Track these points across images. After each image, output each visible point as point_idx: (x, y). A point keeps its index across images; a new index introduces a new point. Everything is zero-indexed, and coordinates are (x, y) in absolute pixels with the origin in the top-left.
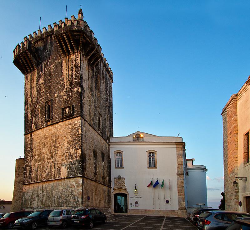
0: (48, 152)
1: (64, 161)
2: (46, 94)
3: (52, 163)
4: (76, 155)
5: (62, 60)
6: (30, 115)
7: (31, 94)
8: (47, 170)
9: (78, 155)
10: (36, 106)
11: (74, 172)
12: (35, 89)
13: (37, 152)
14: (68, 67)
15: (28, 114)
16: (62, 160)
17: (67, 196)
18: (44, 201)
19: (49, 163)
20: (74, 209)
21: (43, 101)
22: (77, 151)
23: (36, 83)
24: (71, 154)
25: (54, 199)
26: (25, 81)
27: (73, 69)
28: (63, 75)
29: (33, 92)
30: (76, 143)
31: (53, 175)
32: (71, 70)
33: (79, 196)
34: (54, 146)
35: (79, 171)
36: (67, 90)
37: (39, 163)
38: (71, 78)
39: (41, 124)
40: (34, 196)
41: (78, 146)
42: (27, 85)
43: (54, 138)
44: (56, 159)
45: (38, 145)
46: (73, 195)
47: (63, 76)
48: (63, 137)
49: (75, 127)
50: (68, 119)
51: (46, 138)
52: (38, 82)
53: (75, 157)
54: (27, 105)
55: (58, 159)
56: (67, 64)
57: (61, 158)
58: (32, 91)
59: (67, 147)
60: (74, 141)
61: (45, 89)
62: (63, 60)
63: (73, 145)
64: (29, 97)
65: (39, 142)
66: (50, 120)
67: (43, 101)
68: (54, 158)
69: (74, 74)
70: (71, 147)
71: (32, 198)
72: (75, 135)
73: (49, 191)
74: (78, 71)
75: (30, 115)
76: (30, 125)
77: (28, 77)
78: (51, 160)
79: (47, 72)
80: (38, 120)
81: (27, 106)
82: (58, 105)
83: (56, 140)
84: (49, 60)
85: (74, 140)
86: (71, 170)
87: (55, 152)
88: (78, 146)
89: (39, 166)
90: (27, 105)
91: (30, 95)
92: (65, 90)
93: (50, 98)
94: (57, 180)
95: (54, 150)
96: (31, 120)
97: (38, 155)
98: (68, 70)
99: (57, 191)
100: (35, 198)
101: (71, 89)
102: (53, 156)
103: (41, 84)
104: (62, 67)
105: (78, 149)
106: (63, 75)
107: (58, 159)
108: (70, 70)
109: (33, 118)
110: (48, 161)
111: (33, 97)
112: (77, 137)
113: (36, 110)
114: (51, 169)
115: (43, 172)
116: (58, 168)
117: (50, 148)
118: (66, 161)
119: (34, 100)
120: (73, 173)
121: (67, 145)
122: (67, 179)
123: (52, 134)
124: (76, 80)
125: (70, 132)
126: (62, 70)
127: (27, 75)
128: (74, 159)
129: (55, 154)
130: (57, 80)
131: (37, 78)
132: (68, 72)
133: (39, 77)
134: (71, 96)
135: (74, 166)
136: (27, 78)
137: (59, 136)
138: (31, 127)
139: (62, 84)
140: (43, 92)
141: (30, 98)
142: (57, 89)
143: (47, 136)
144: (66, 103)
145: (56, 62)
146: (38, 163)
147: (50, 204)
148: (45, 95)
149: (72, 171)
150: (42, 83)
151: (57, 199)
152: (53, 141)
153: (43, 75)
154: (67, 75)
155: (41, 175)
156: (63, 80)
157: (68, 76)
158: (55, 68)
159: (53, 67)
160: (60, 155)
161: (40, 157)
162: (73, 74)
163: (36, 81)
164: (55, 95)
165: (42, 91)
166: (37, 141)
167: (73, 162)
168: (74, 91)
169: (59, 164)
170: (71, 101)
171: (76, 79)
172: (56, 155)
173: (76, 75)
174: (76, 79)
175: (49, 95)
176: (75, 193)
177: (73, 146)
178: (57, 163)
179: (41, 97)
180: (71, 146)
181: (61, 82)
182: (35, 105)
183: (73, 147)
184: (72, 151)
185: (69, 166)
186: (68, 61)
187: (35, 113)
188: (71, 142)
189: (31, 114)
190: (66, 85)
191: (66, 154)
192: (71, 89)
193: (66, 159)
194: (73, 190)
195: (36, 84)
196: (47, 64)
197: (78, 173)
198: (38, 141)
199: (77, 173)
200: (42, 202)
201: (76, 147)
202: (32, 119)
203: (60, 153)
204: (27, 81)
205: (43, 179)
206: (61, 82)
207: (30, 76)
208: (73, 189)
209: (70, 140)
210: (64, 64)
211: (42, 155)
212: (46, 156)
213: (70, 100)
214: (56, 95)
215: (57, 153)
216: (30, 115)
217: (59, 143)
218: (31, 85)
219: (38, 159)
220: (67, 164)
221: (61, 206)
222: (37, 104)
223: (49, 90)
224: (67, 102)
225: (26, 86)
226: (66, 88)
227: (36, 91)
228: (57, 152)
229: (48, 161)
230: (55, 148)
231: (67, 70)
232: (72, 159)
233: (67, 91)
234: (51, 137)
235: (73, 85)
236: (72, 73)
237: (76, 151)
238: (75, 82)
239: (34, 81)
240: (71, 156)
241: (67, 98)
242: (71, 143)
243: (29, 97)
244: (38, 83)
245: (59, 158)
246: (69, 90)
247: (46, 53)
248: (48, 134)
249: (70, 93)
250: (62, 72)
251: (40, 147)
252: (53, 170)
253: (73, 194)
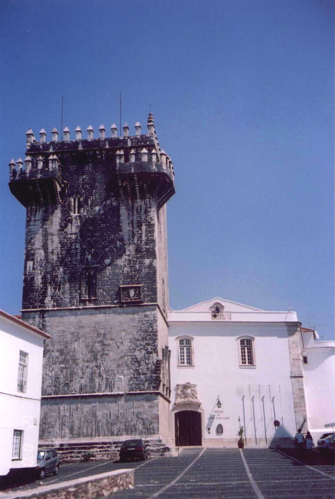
0: (85, 351)
1: (122, 368)
2: (83, 254)
3: (95, 368)
4: (147, 361)
5: (119, 204)
6: (38, 280)
7: (43, 244)
8: (82, 378)
9: (151, 361)
10: (59, 269)
11: (144, 385)
12: (56, 239)
13: (57, 347)
14: (131, 219)
15: (34, 277)
16: (119, 366)
17: (130, 419)
18: (76, 428)
19: (87, 367)
20: (146, 438)
21: (76, 265)
22: (151, 355)
23: (58, 228)
24: (137, 359)
25: (100, 424)
26: (28, 216)
27: (142, 226)
28: (121, 231)
29: (49, 242)
30: (148, 344)
31: (97, 386)
32: (137, 226)
33: (153, 421)
34: (101, 342)
35: (153, 385)
36: (131, 258)
37: (63, 366)
38: (138, 241)
39: (70, 302)
40: (49, 420)
41: (151, 348)
42: (34, 225)
43: (100, 330)
44: (105, 363)
45: (59, 334)
46: (141, 418)
47: (121, 233)
48: (120, 331)
49: (146, 319)
50: (133, 306)
51: (81, 327)
52: (63, 228)
53: (146, 363)
54: (33, 260)
55: (110, 363)
56: (129, 214)
57: (116, 363)
58: (47, 240)
59: (130, 347)
60: (143, 340)
61: (81, 246)
62: (121, 205)
63: (141, 345)
64: (39, 249)
65: (63, 331)
66: (93, 299)
67: (76, 265)
68: (99, 361)
69: (144, 235)
70: (138, 349)
71: (45, 423)
72: (146, 331)
73: (87, 412)
74: (151, 231)
75: (40, 281)
76: (39, 297)
77: (36, 211)
78: (93, 364)
79: (86, 216)
80: (63, 293)
81: (30, 264)
82: (111, 280)
83: (105, 334)
84: (91, 195)
85: (144, 339)
86: (137, 382)
87: (102, 352)
88: (151, 348)
89: (62, 371)
90: (33, 260)
91: (43, 246)
92: (127, 258)
93: (94, 264)
94: (107, 395)
95: (100, 349)
96: (42, 289)
97: (61, 352)
98: (133, 226)
99: (105, 412)
100: (53, 423)
101: (138, 258)
102: (99, 357)
103: (71, 234)
104: (119, 216)
105: (151, 353)
106: (121, 231)
107: (110, 363)
108: (135, 225)
109: (49, 288)
110: (86, 364)
111: (50, 250)
112: (150, 335)
113: (57, 276)
114: (92, 377)
115: (71, 381)
116: (108, 377)
117: (91, 344)
118: (126, 368)
119: (55, 257)
120: (142, 387)
121: (129, 344)
122: (129, 396)
123: (96, 323)
124: (148, 247)
125: (135, 325)
126: (119, 222)
127: (34, 207)
128: (143, 368)
129: (102, 356)
130: (109, 236)
131: (61, 219)
132: (131, 228)
133: (65, 220)
134: (139, 271)
135: (142, 377)
136: (34, 213)
137: (111, 328)
138: (42, 301)
139: (120, 245)
140: (77, 249)
141: (42, 252)
142: (109, 251)
143: (84, 325)
144: (127, 279)
145: (106, 204)
146: (60, 364)
147: (92, 432)
148: (81, 256)
149: (140, 384)
150: (75, 234)
151: (107, 424)
152: (98, 334)
153: (76, 218)
154: (131, 233)
155: (67, 385)
156: (122, 240)
157: (131, 236)
158: (102, 214)
159: (100, 210)
160: (115, 357)
161: (66, 356)
162: (141, 234)
163: (58, 224)
164: (104, 261)
165: (73, 247)
166: (58, 328)
167: (141, 371)
168: (145, 263)
169: (112, 370)
170: (138, 278)
171: (146, 244)
172: (104, 356)
173: (148, 238)
174: (146, 244)
175: (89, 257)
176: (145, 416)
177: (142, 347)
178: (107, 369)
179: (69, 256)
180: (138, 346)
181: (118, 243)
182: (55, 266)
183: (141, 349)
184: (139, 355)
185: (132, 376)
186: (131, 210)
187: (54, 280)
188: (138, 340)
189: (42, 278)
190: (129, 250)
191: (126, 358)
192: (138, 258)
193: (127, 365)
194: (140, 413)
195: (60, 230)
196: (86, 201)
197: (151, 387)
198: (62, 328)
199: (149, 387)
200: (72, 430)
201: (147, 349)
202: (46, 289)
203: (112, 355)
204: (33, 218)
205: (74, 392)
206: (118, 243)
207: (41, 212)
208: (141, 410)
209: (137, 337)
210: (123, 210)
211: (71, 354)
212: (79, 356)
213: (136, 276)
214: (107, 261)
215: (106, 355)
216: (38, 280)
217: (112, 339)
218: (46, 228)
219: (60, 357)
220: (129, 372)
221: (117, 435)
222: (61, 266)
223: (91, 249)
224: (131, 279)
225: (30, 227)
226: (129, 255)
227: (60, 243)
228: (106, 352)
229: (86, 364)
230: (101, 345)
231: (129, 223)
232: (139, 366)
233: (130, 260)
234: (95, 327)
235: (142, 252)
236: (140, 232)
237: (147, 355)
238: (146, 248)
239: (53, 223)
240: (139, 362)
241: (131, 272)
242: (138, 342)
243: (39, 249)
244: (63, 230)
245: (111, 361)
246: (135, 259)
247: (84, 180)
248: (86, 322)
249: (136, 264)
250: (121, 226)
251: (65, 339)
252: (97, 380)
253: (141, 417)
